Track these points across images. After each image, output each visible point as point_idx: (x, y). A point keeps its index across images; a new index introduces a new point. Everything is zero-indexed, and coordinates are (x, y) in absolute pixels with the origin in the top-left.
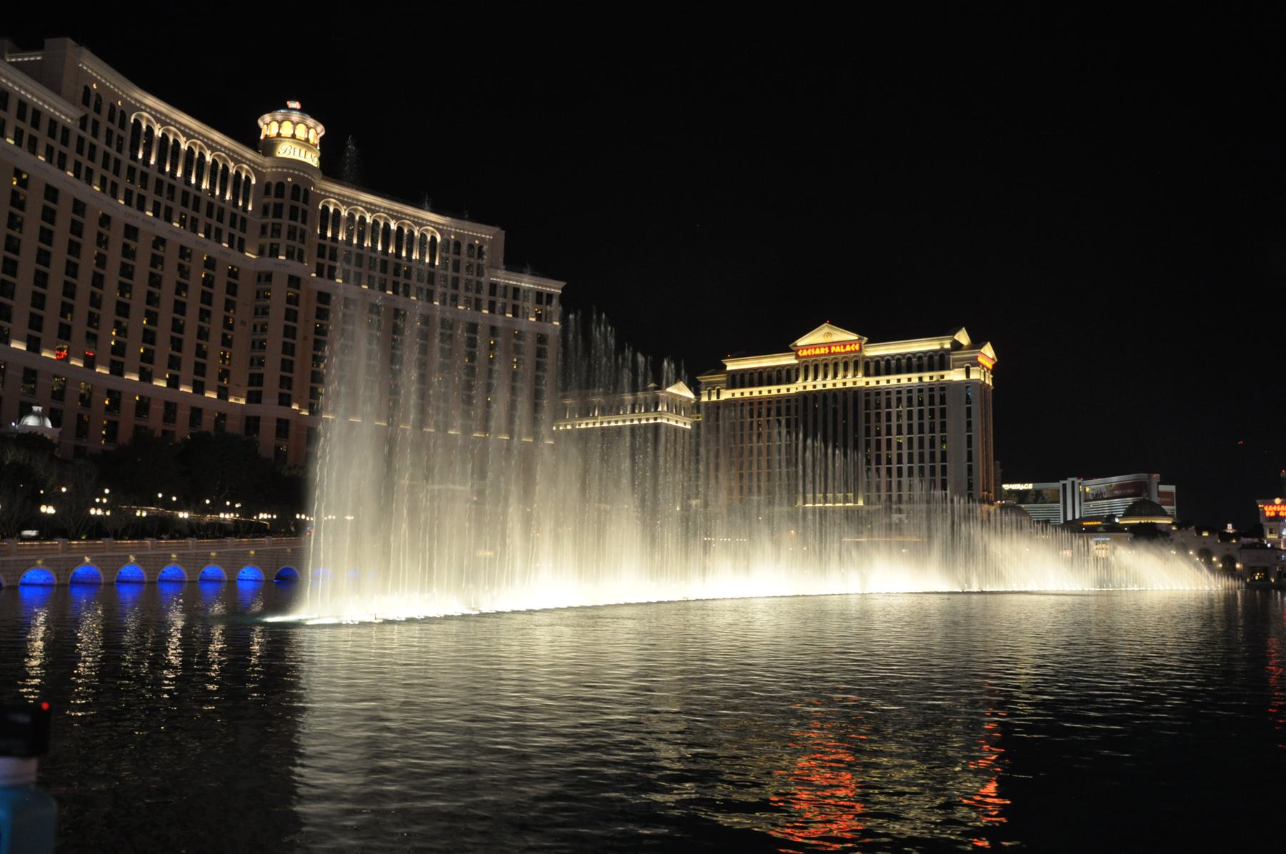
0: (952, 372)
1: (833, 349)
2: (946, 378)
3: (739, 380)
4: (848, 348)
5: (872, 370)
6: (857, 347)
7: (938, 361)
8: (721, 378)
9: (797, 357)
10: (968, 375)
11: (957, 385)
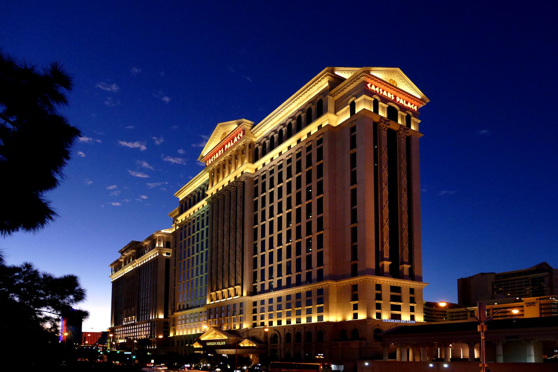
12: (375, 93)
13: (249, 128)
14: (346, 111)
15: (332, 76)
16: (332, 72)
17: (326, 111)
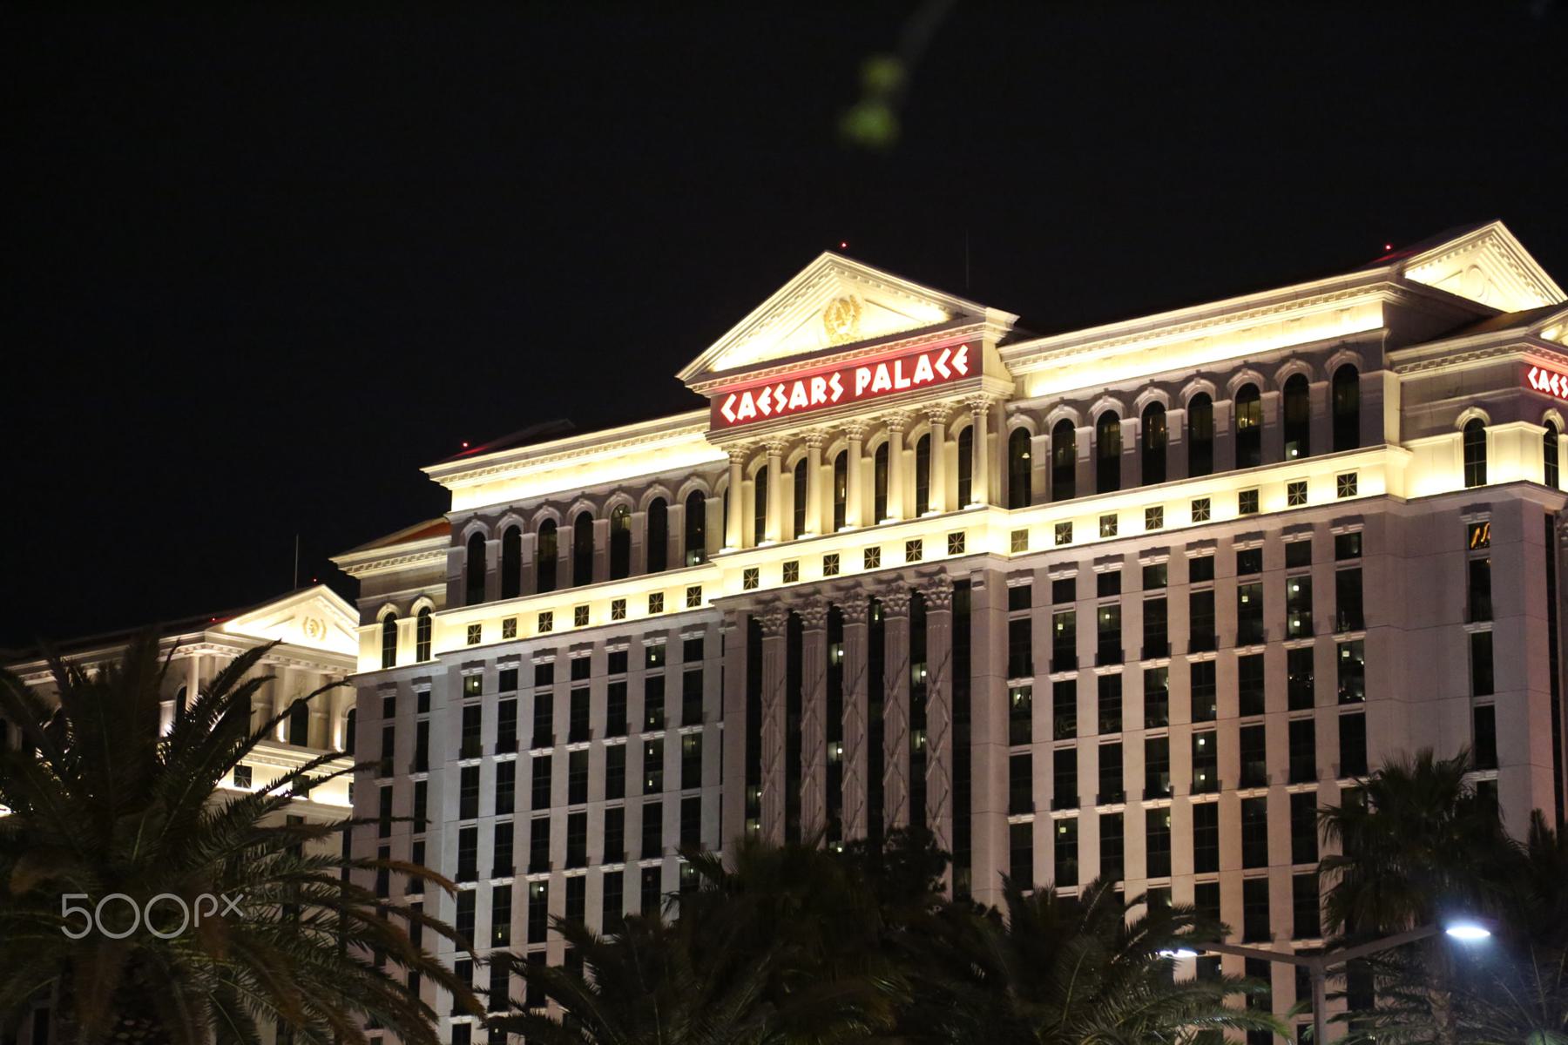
1: (862, 378)
2: (1367, 487)
3: (505, 561)
6: (960, 362)
7: (1324, 405)
8: (427, 555)
9: (719, 428)
12: (1550, 404)
13: (997, 337)
14: (1450, 446)
15: (1396, 290)
16: (1401, 274)
17: (1376, 439)
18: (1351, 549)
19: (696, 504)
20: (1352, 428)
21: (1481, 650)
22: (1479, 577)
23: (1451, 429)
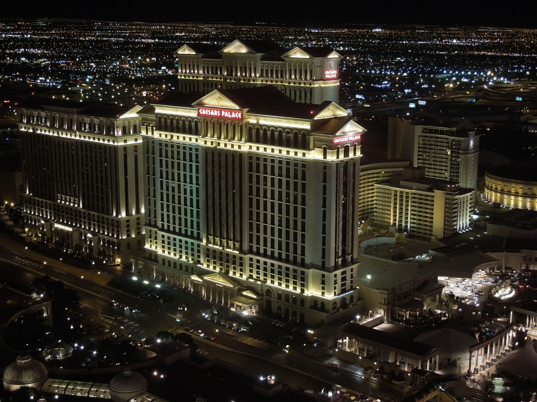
0: (312, 152)
1: (223, 113)
4: (233, 115)
5: (254, 137)
10: (325, 157)
11: (316, 163)
18: (305, 164)
19: (196, 123)
20: (305, 146)
21: (325, 187)
22: (325, 174)
23: (322, 148)
